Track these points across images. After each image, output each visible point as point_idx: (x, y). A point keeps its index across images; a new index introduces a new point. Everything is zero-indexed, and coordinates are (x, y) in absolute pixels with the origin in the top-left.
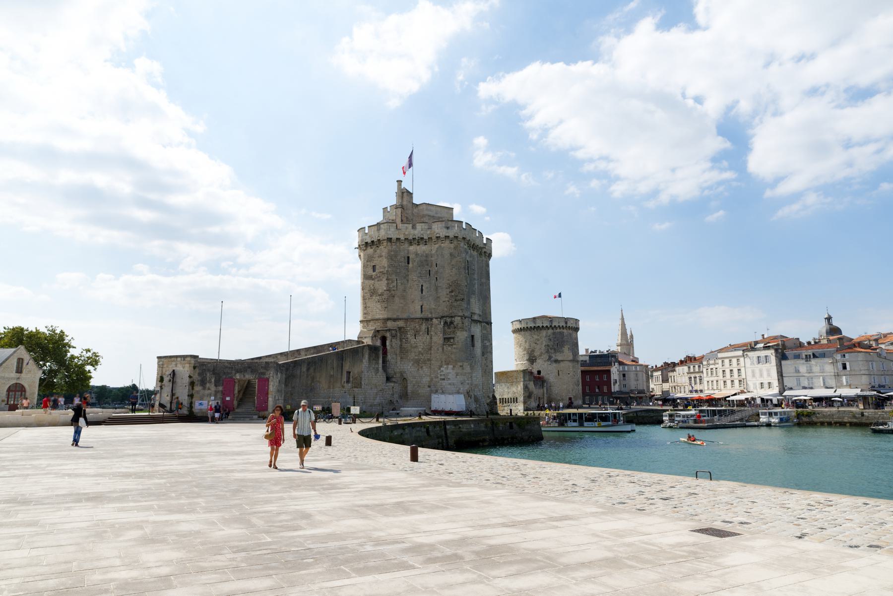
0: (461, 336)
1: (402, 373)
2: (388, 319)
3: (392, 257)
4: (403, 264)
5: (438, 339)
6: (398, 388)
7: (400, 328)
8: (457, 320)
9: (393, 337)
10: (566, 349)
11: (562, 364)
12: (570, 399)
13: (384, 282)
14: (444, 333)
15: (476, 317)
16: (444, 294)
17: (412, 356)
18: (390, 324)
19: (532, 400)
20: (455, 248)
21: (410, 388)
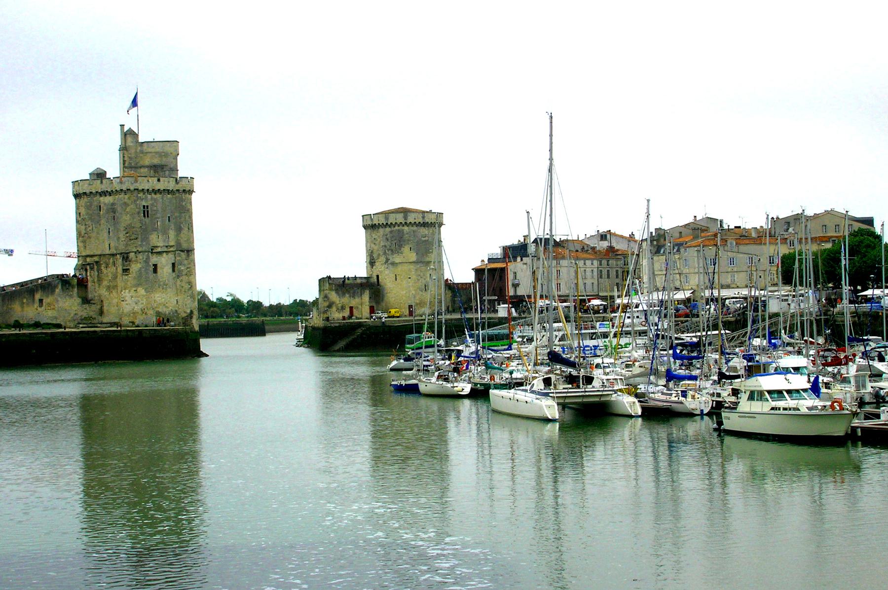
0: (135, 267)
1: (100, 296)
2: (87, 256)
3: (89, 207)
4: (96, 212)
5: (120, 270)
6: (96, 308)
7: (97, 262)
8: (132, 255)
9: (92, 269)
10: (406, 249)
11: (400, 269)
12: (410, 307)
13: (83, 227)
14: (123, 265)
15: (159, 250)
16: (122, 235)
17: (105, 283)
18: (88, 260)
19: (334, 309)
20: (129, 198)
21: (105, 308)
